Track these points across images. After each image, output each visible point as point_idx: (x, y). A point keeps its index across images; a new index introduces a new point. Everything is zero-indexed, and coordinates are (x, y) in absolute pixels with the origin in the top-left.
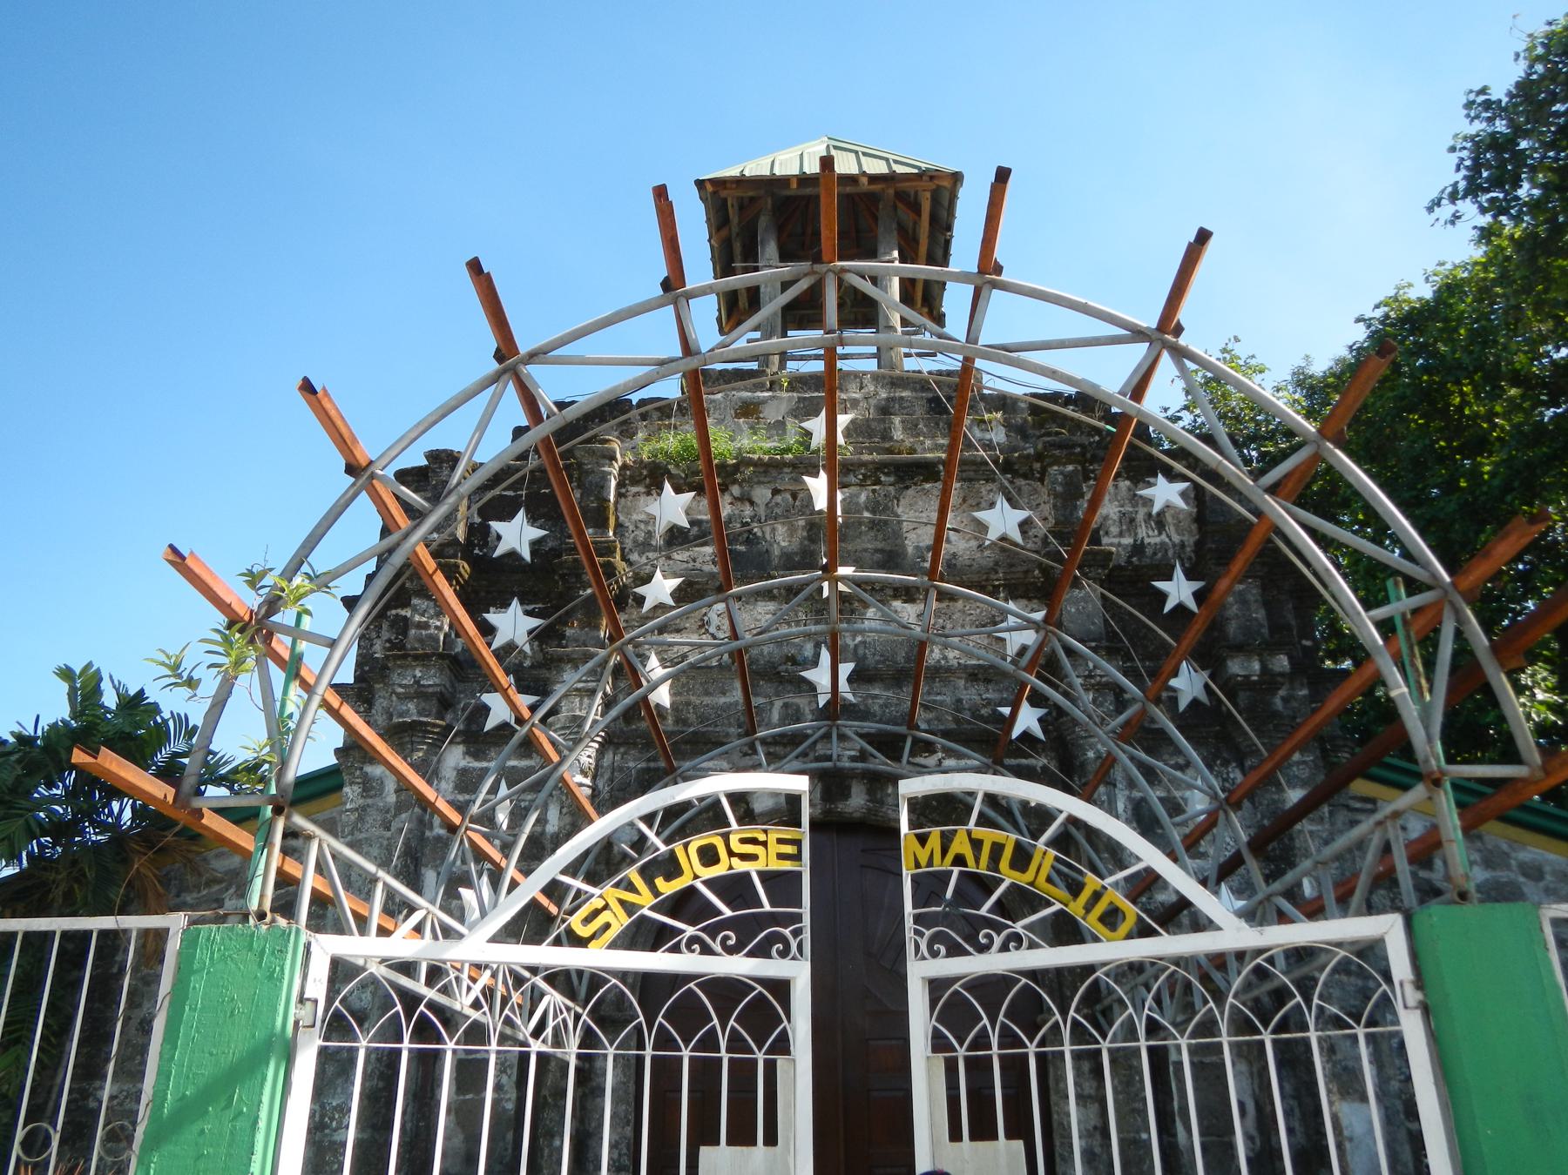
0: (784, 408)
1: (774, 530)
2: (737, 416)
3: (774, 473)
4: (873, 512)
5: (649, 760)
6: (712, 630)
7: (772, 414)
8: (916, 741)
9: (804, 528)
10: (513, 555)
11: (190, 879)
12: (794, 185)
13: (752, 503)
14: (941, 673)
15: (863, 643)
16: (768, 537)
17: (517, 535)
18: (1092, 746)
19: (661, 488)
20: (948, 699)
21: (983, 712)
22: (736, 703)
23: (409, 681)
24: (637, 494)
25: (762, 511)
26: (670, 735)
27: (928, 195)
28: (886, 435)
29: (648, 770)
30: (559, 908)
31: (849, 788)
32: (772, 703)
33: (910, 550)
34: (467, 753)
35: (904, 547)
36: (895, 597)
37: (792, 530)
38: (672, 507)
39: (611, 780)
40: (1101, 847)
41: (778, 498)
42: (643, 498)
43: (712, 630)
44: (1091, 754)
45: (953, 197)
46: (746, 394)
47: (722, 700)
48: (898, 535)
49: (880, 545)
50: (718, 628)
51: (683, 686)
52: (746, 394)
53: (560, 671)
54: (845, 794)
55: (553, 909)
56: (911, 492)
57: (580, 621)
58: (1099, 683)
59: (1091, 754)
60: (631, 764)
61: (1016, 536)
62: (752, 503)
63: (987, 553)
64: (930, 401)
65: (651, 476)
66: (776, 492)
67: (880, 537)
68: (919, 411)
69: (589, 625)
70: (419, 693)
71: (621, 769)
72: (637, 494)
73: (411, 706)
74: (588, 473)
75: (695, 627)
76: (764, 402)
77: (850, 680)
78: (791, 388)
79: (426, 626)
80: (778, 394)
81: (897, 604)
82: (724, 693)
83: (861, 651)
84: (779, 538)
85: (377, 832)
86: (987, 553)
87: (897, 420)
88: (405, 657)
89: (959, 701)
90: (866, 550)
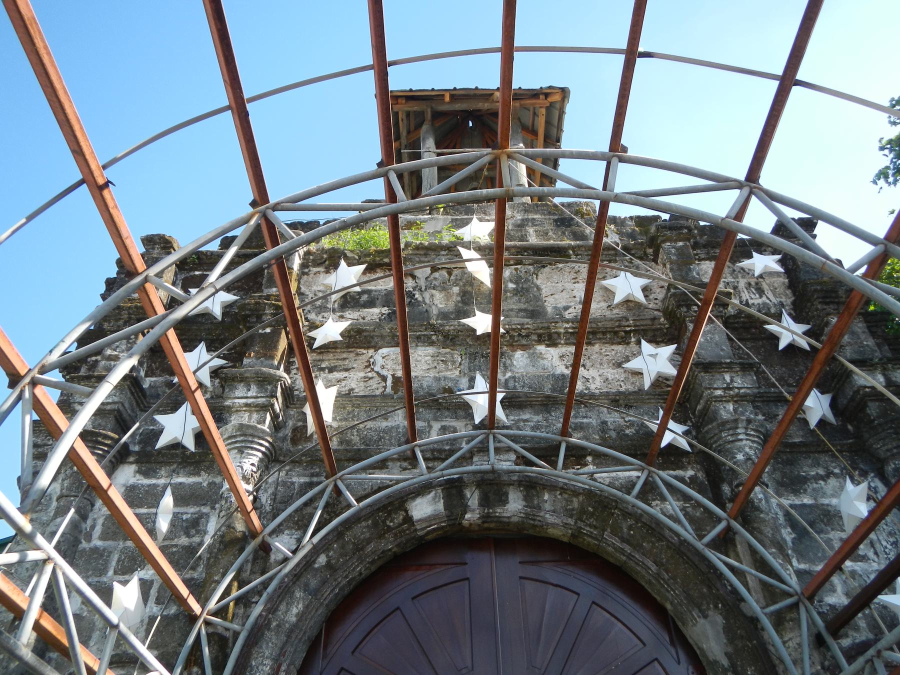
1: (432, 296)
3: (431, 253)
4: (516, 283)
5: (312, 475)
6: (377, 368)
8: (570, 448)
9: (458, 295)
12: (447, 99)
14: (589, 400)
15: (514, 378)
16: (427, 301)
18: (740, 450)
20: (593, 421)
21: (627, 432)
22: (398, 427)
24: (319, 272)
25: (422, 283)
26: (336, 451)
27: (543, 111)
30: (203, 607)
31: (506, 494)
32: (430, 427)
33: (549, 310)
35: (544, 308)
36: (540, 341)
37: (448, 297)
38: (348, 276)
39: (275, 494)
40: (768, 542)
41: (436, 275)
43: (377, 368)
44: (740, 457)
45: (562, 113)
47: (384, 424)
48: (538, 298)
49: (523, 306)
51: (349, 413)
54: (503, 500)
55: (196, 608)
56: (547, 269)
57: (257, 353)
58: (737, 395)
59: (740, 457)
60: (294, 479)
61: (640, 296)
63: (615, 311)
66: (434, 269)
67: (523, 300)
69: (265, 356)
71: (284, 483)
72: (319, 272)
77: (501, 402)
80: (436, 216)
81: (541, 348)
82: (386, 419)
83: (511, 384)
84: (436, 302)
86: (615, 311)
89: (604, 423)
90: (512, 310)
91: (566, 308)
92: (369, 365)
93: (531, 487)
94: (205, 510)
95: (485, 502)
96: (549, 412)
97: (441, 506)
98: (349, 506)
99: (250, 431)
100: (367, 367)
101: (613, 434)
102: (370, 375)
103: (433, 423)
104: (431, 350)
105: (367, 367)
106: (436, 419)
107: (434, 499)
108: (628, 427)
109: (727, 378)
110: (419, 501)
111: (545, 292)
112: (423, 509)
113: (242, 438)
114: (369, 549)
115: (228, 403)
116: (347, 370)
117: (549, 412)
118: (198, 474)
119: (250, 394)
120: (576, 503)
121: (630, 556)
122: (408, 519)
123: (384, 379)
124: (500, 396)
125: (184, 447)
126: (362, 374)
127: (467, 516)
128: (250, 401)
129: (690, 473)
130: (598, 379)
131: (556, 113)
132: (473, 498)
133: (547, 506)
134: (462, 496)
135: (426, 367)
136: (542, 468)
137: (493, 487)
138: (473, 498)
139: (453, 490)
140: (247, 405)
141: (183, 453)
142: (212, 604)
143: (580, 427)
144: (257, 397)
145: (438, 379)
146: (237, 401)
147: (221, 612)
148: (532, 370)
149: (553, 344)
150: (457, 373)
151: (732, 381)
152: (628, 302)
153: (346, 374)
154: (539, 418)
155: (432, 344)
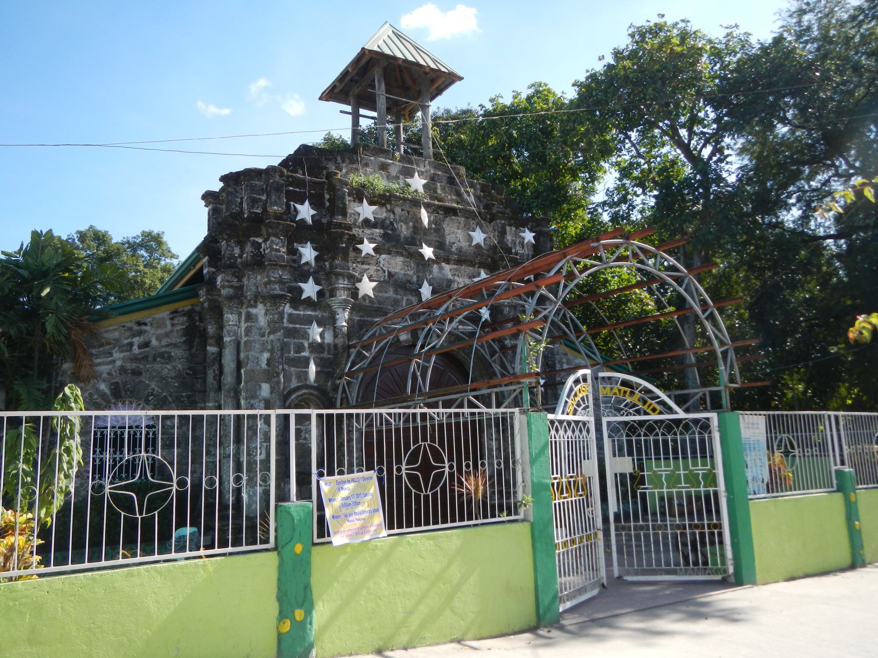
0: (397, 169)
2: (380, 169)
7: (394, 171)
10: (303, 221)
11: (95, 343)
12: (400, 62)
13: (394, 213)
17: (306, 212)
19: (361, 201)
23: (277, 276)
25: (397, 217)
28: (435, 192)
29: (361, 321)
34: (291, 307)
37: (408, 228)
42: (352, 203)
45: (452, 82)
46: (383, 160)
47: (386, 295)
48: (443, 236)
52: (383, 160)
53: (338, 279)
62: (394, 213)
64: (448, 178)
65: (359, 194)
66: (402, 210)
68: (445, 181)
70: (281, 282)
73: (277, 286)
74: (338, 190)
76: (389, 165)
78: (400, 161)
79: (278, 251)
81: (443, 264)
85: (257, 337)
87: (439, 185)
88: (276, 265)
91: (454, 243)
104: (402, 259)
111: (447, 232)
116: (369, 264)
118: (315, 311)
123: (384, 272)
131: (449, 81)
145: (405, 275)
148: (440, 275)
149: (448, 263)
152: (478, 246)
155: (403, 256)
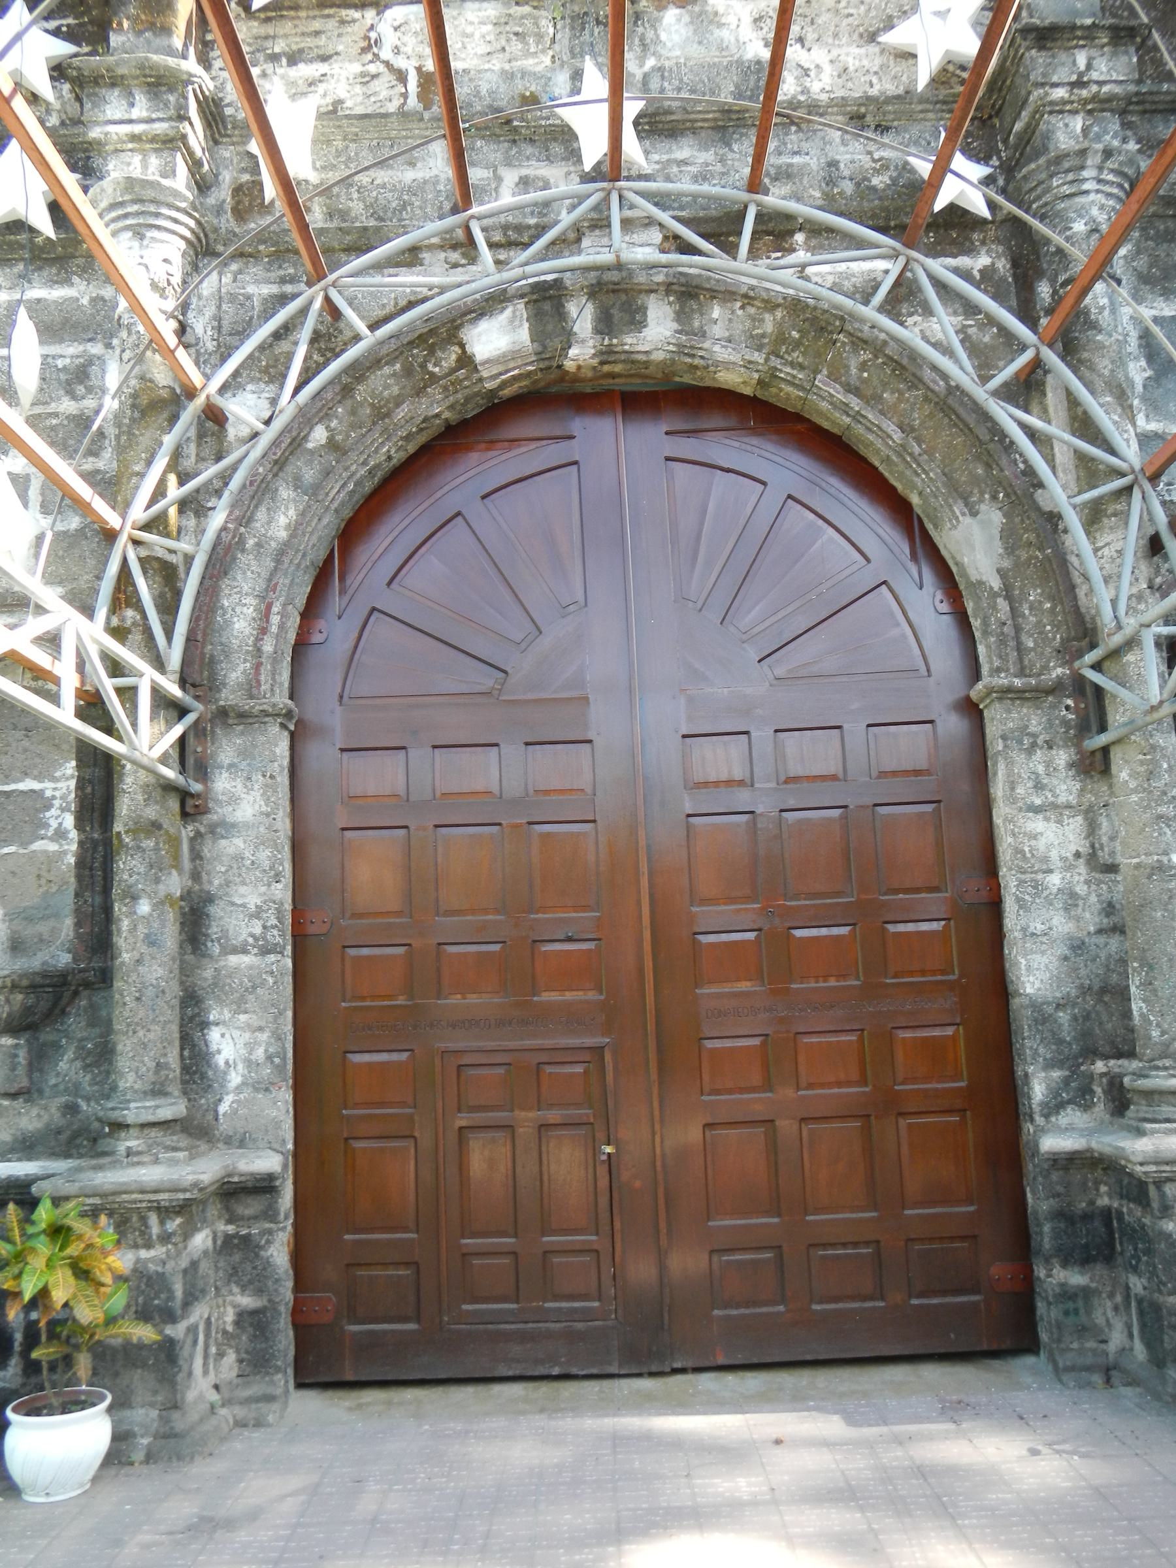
5: (283, 281)
6: (386, 54)
14: (805, 116)
15: (660, 69)
18: (1081, 212)
21: (876, 181)
22: (436, 181)
26: (321, 231)
30: (124, 516)
31: (643, 310)
32: (499, 179)
39: (218, 319)
40: (1099, 385)
43: (386, 54)
44: (1079, 227)
47: (410, 176)
50: (397, 51)
51: (338, 154)
54: (636, 319)
55: (113, 519)
57: (134, 20)
58: (1095, 98)
59: (1079, 227)
60: (251, 289)
69: (152, 26)
71: (233, 298)
75: (355, 50)
77: (636, 123)
82: (412, 164)
83: (655, 84)
89: (833, 164)
92: (369, 46)
93: (688, 294)
94: (96, 349)
95: (605, 325)
96: (728, 145)
97: (523, 335)
98: (357, 338)
99: (149, 193)
100: (365, 50)
101: (848, 187)
102: (372, 68)
103: (503, 172)
105: (365, 50)
106: (509, 163)
107: (511, 321)
108: (877, 172)
109: (1081, 59)
110: (484, 325)
112: (497, 341)
113: (135, 208)
114: (401, 413)
115: (95, 133)
116: (324, 58)
117: (728, 145)
119: (136, 113)
120: (769, 324)
121: (857, 417)
122: (466, 360)
123: (402, 77)
124: (632, 109)
125: (32, 230)
126: (356, 68)
127: (573, 352)
128: (138, 129)
129: (984, 260)
130: (828, 69)
132: (582, 316)
133: (718, 331)
134: (560, 314)
135: (483, 49)
136: (711, 261)
137: (618, 296)
138: (582, 316)
139: (546, 300)
140: (134, 138)
141: (31, 240)
142: (138, 512)
143: (785, 174)
144: (150, 121)
145: (508, 76)
146: (111, 128)
147: (156, 524)
148: (696, 52)
150: (547, 61)
151: (1089, 66)
153: (323, 68)
154: (708, 156)
